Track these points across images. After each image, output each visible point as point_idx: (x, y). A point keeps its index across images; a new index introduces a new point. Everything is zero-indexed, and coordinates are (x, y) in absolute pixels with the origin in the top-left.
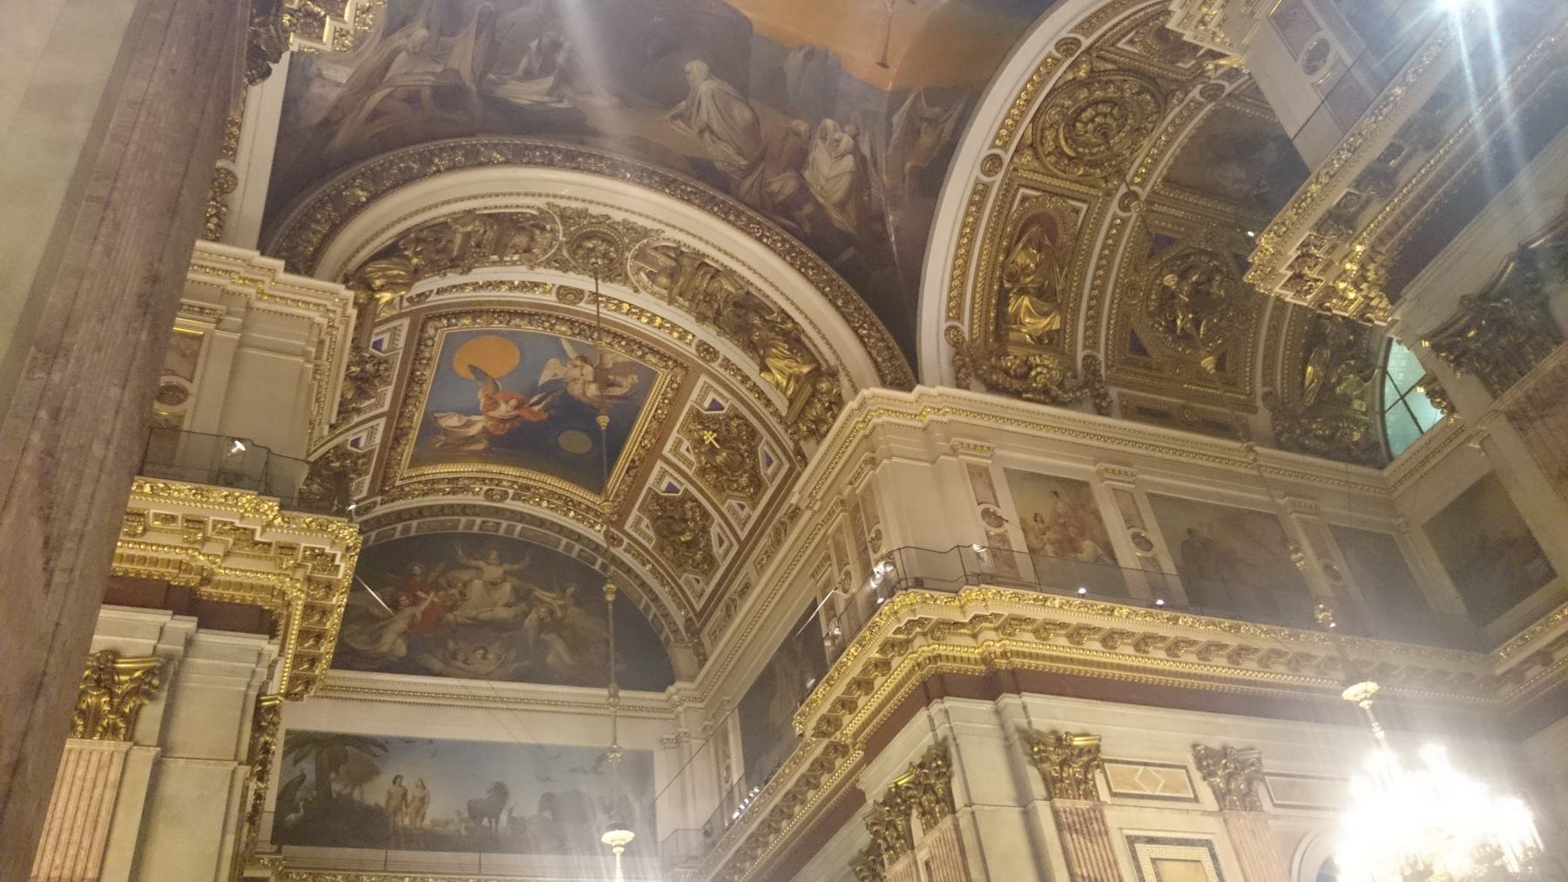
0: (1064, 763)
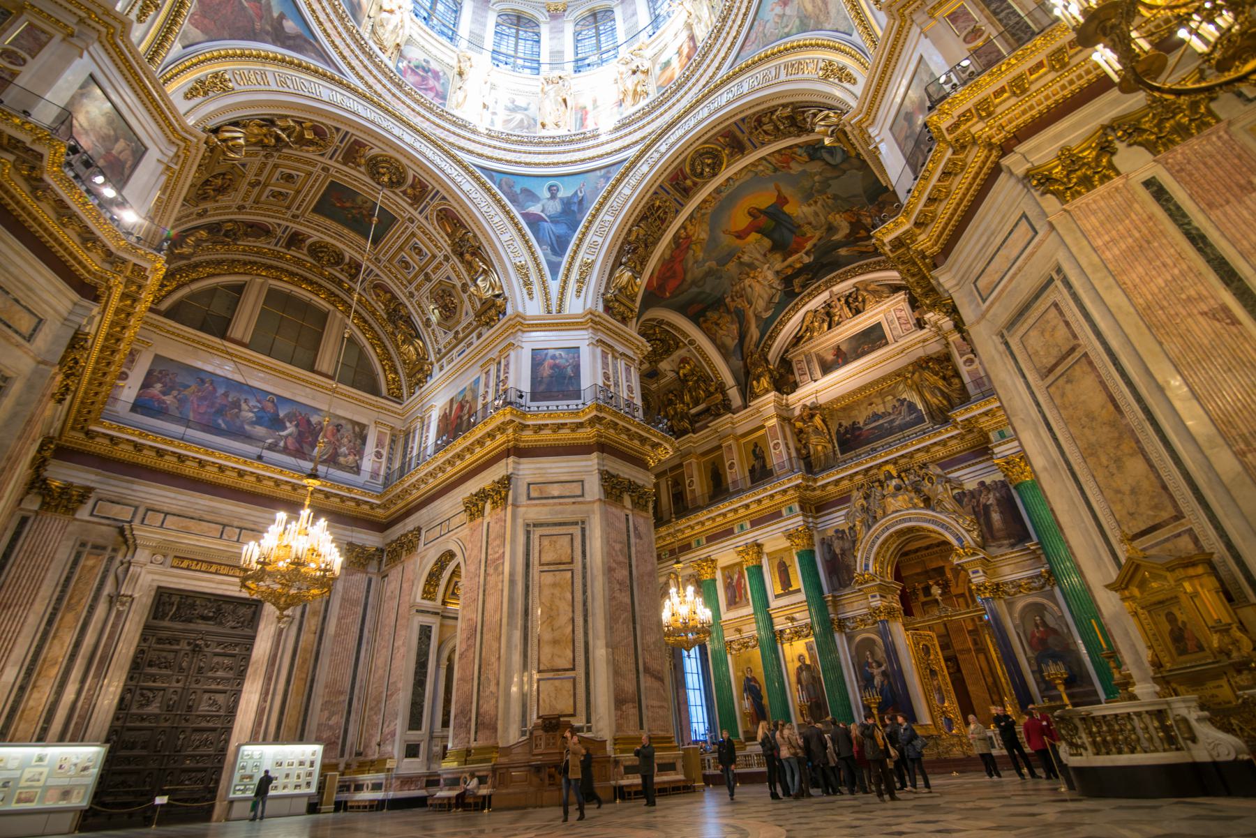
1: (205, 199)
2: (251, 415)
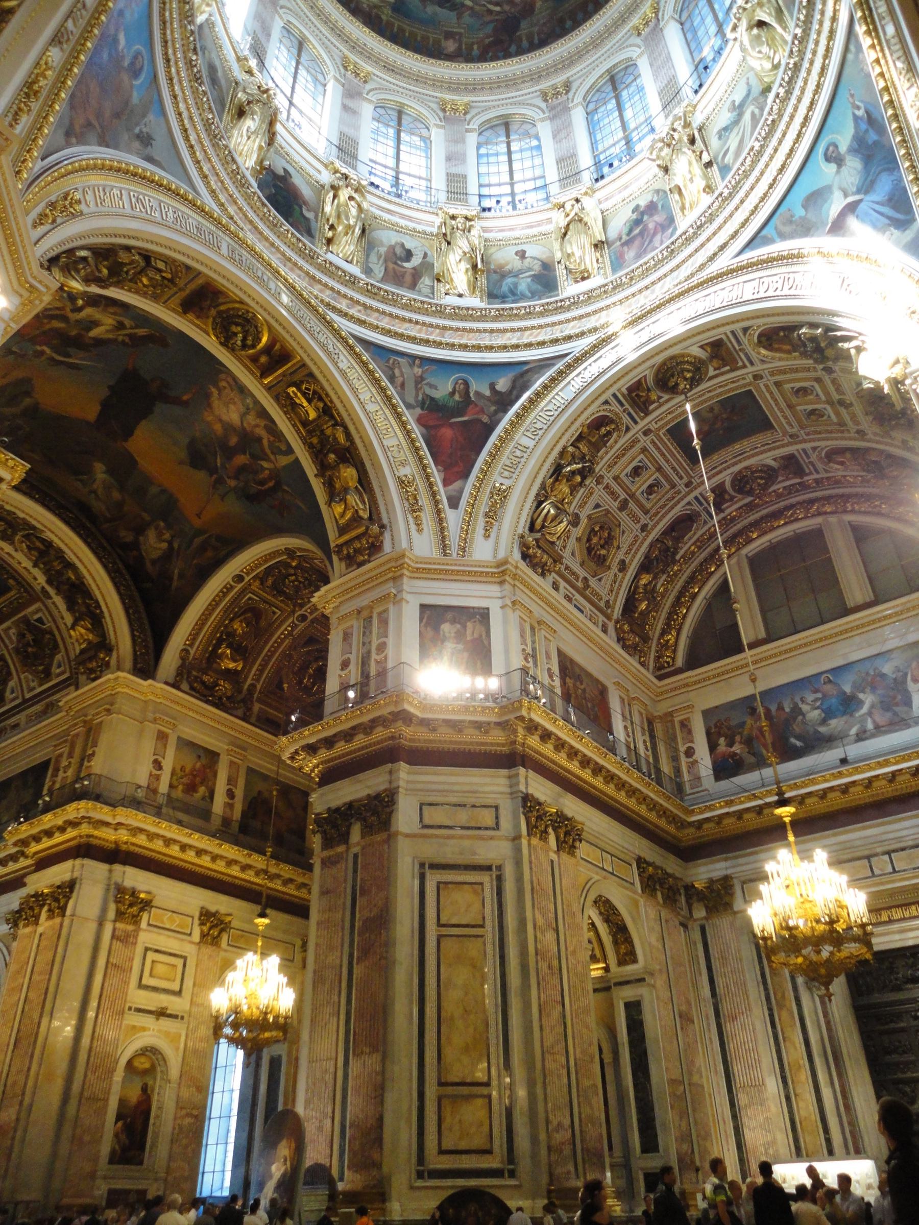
0: (131, 905)
1: (605, 560)
2: (816, 713)
